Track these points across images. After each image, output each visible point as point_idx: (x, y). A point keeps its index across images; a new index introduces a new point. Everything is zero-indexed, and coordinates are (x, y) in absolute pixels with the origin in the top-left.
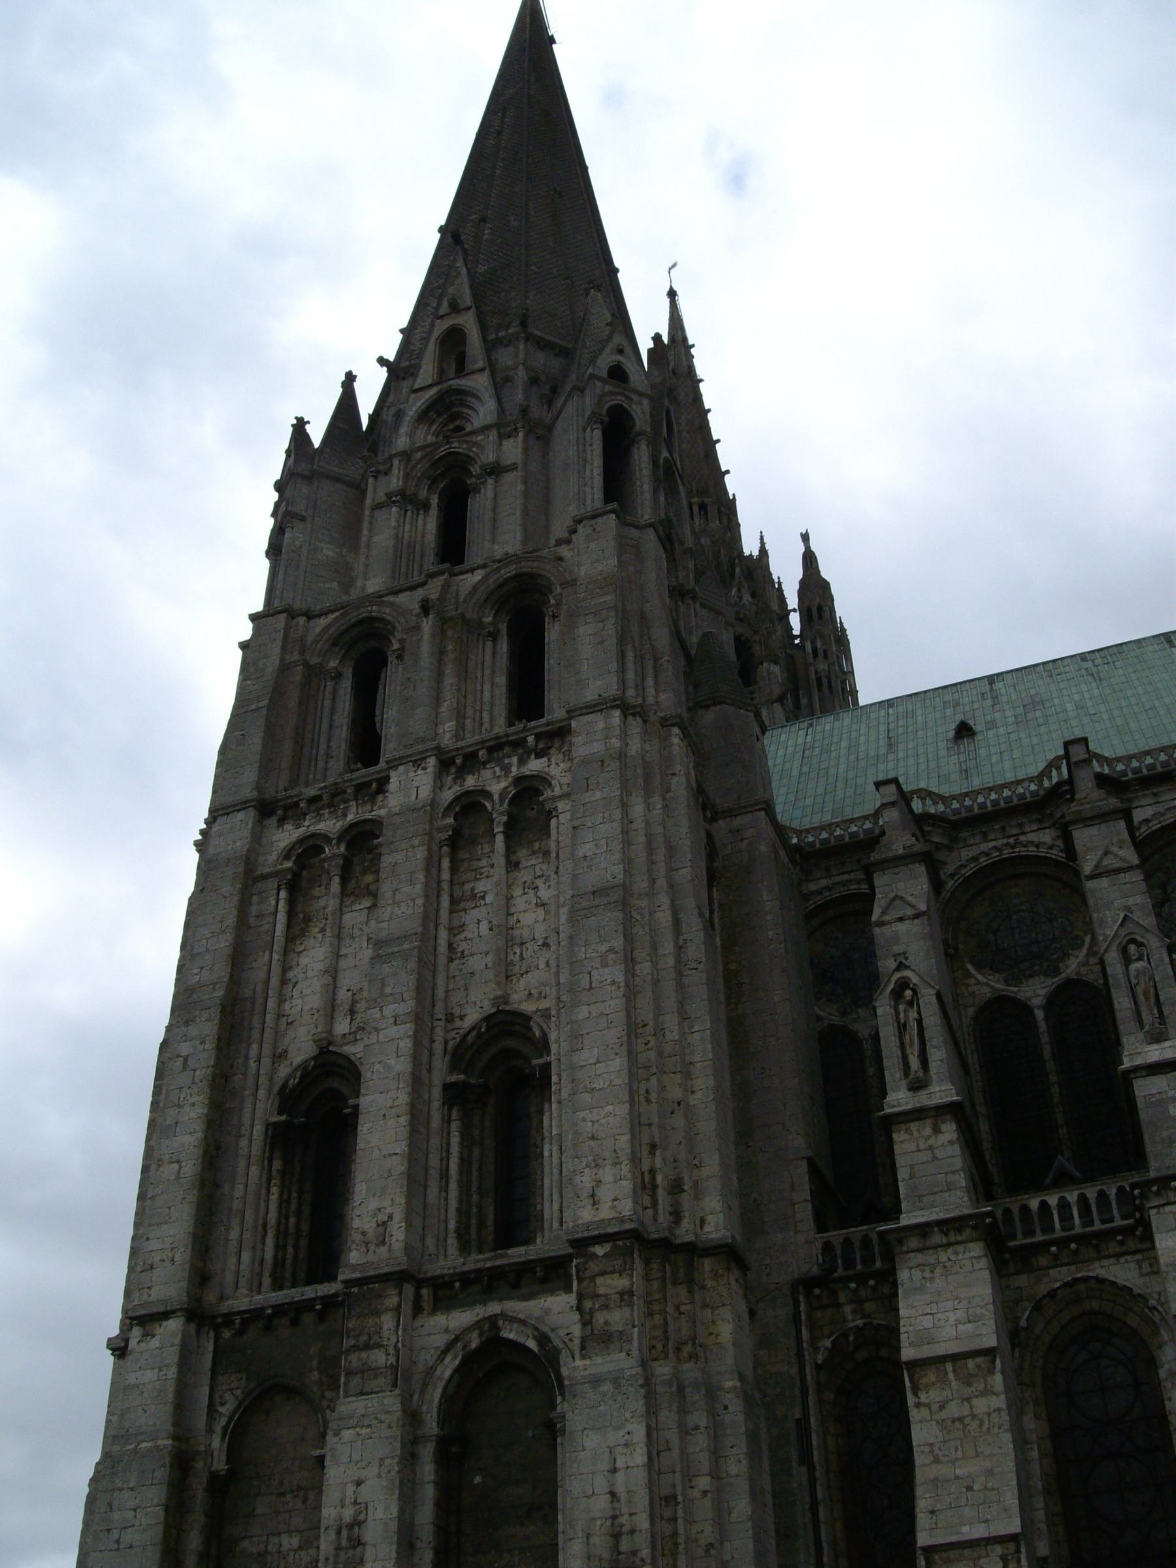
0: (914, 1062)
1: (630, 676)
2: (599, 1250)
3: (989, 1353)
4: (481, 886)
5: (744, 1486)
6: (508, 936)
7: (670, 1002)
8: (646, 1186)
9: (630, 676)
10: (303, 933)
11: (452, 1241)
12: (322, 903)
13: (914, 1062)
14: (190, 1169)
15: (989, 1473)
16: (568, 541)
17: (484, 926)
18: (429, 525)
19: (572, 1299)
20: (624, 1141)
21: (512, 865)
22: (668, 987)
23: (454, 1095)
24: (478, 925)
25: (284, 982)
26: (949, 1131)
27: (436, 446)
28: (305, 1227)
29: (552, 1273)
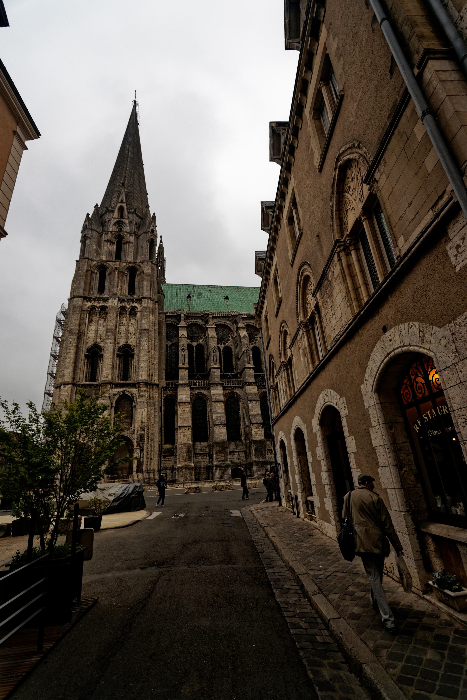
0: (183, 360)
1: (151, 293)
2: (142, 384)
3: (189, 402)
4: (124, 322)
5: (158, 417)
6: (127, 331)
7: (153, 348)
8: (149, 375)
9: (151, 293)
10: (91, 322)
11: (117, 378)
12: (95, 318)
13: (183, 360)
14: (72, 361)
15: (187, 418)
16: (142, 263)
17: (124, 329)
18: (114, 248)
19: (137, 390)
20: (146, 369)
21: (130, 320)
22: (153, 345)
23: (118, 355)
24: (123, 328)
25: (88, 330)
26: (187, 371)
27: (117, 232)
28: (90, 371)
29: (134, 385)
